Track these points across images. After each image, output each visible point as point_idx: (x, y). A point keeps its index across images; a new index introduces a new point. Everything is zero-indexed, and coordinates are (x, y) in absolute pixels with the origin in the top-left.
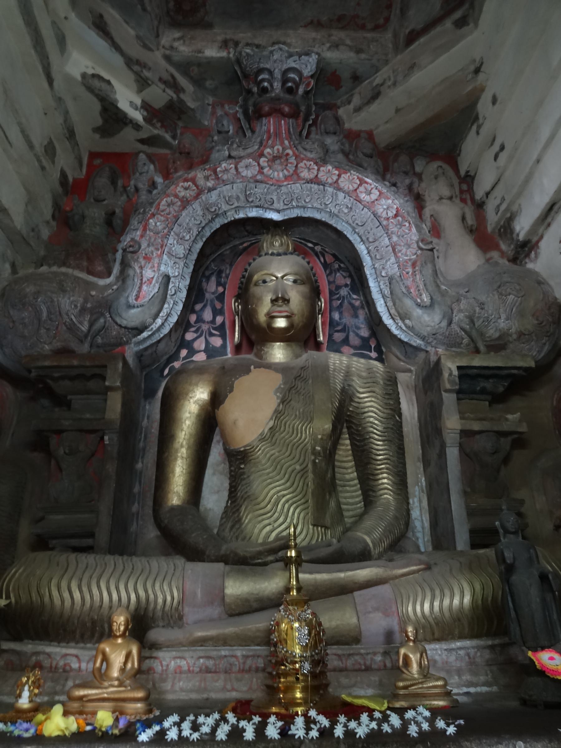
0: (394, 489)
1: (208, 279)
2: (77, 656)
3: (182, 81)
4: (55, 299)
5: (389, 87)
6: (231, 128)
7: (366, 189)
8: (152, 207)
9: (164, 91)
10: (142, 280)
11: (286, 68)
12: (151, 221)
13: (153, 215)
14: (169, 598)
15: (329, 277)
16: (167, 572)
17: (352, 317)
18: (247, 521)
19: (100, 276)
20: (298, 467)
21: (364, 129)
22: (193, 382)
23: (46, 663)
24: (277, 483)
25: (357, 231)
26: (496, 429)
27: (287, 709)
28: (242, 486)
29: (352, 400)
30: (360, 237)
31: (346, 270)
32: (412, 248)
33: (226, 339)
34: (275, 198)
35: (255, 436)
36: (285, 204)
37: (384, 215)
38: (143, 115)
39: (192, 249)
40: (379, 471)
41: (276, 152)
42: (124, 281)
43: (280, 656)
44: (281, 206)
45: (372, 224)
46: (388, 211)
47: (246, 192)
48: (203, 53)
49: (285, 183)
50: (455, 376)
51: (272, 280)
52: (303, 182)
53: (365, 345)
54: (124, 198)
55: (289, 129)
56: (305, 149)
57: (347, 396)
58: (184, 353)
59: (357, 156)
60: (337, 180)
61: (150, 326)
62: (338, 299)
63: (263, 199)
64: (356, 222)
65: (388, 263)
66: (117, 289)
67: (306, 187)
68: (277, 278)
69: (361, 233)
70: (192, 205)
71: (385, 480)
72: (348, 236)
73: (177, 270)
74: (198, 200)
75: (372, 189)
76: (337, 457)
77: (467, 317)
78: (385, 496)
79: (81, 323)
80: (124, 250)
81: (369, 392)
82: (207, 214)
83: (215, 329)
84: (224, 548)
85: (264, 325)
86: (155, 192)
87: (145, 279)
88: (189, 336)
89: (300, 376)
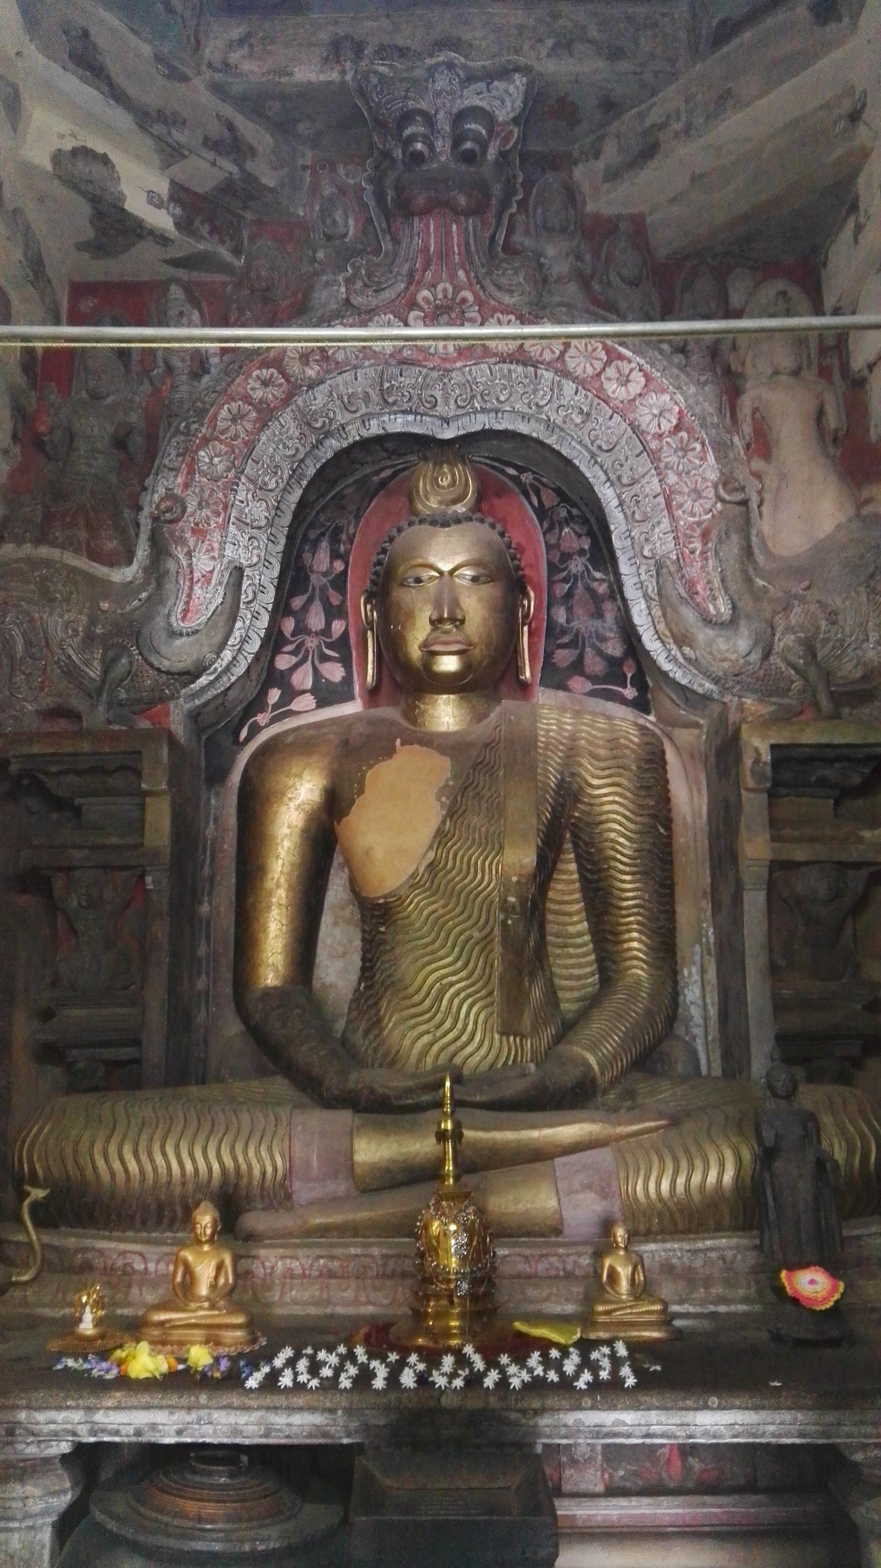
0: (650, 960)
1: (315, 545)
2: (141, 1254)
3: (250, 130)
4: (36, 616)
5: (676, 134)
6: (351, 222)
7: (619, 371)
8: (202, 425)
9: (214, 164)
10: (192, 579)
11: (462, 106)
12: (202, 453)
13: (206, 441)
14: (269, 1169)
15: (548, 536)
16: (264, 1129)
17: (592, 616)
18: (390, 1025)
19: (112, 562)
20: (477, 935)
21: (625, 211)
22: (294, 770)
23: (98, 1262)
24: (441, 963)
25: (599, 460)
26: (836, 857)
27: (436, 1342)
28: (383, 962)
29: (579, 801)
30: (606, 472)
31: (585, 521)
32: (705, 498)
33: (351, 667)
34: (438, 394)
35: (404, 878)
36: (459, 407)
37: (653, 429)
38: (173, 216)
39: (283, 507)
40: (625, 928)
41: (440, 296)
42: (160, 584)
43: (429, 1271)
44: (451, 410)
45: (628, 448)
46: (662, 419)
47: (382, 385)
48: (291, 74)
49: (459, 364)
50: (765, 763)
51: (431, 578)
52: (493, 360)
53: (615, 671)
54: (146, 388)
55: (467, 244)
56: (499, 287)
57: (569, 793)
58: (274, 695)
59: (609, 283)
60: (563, 354)
61: (210, 665)
62: (565, 580)
63: (415, 398)
64: (598, 442)
65: (657, 530)
66: (149, 598)
67: (501, 370)
68: (441, 573)
69: (608, 464)
70: (277, 419)
72: (583, 468)
73: (255, 551)
74: (288, 409)
75: (631, 370)
76: (551, 894)
77: (800, 641)
78: (634, 971)
79: (87, 663)
80: (156, 519)
81: (609, 785)
82: (307, 433)
83: (330, 646)
84: (354, 1076)
85: (419, 664)
86: (206, 379)
87: (197, 575)
88: (283, 662)
89: (482, 762)
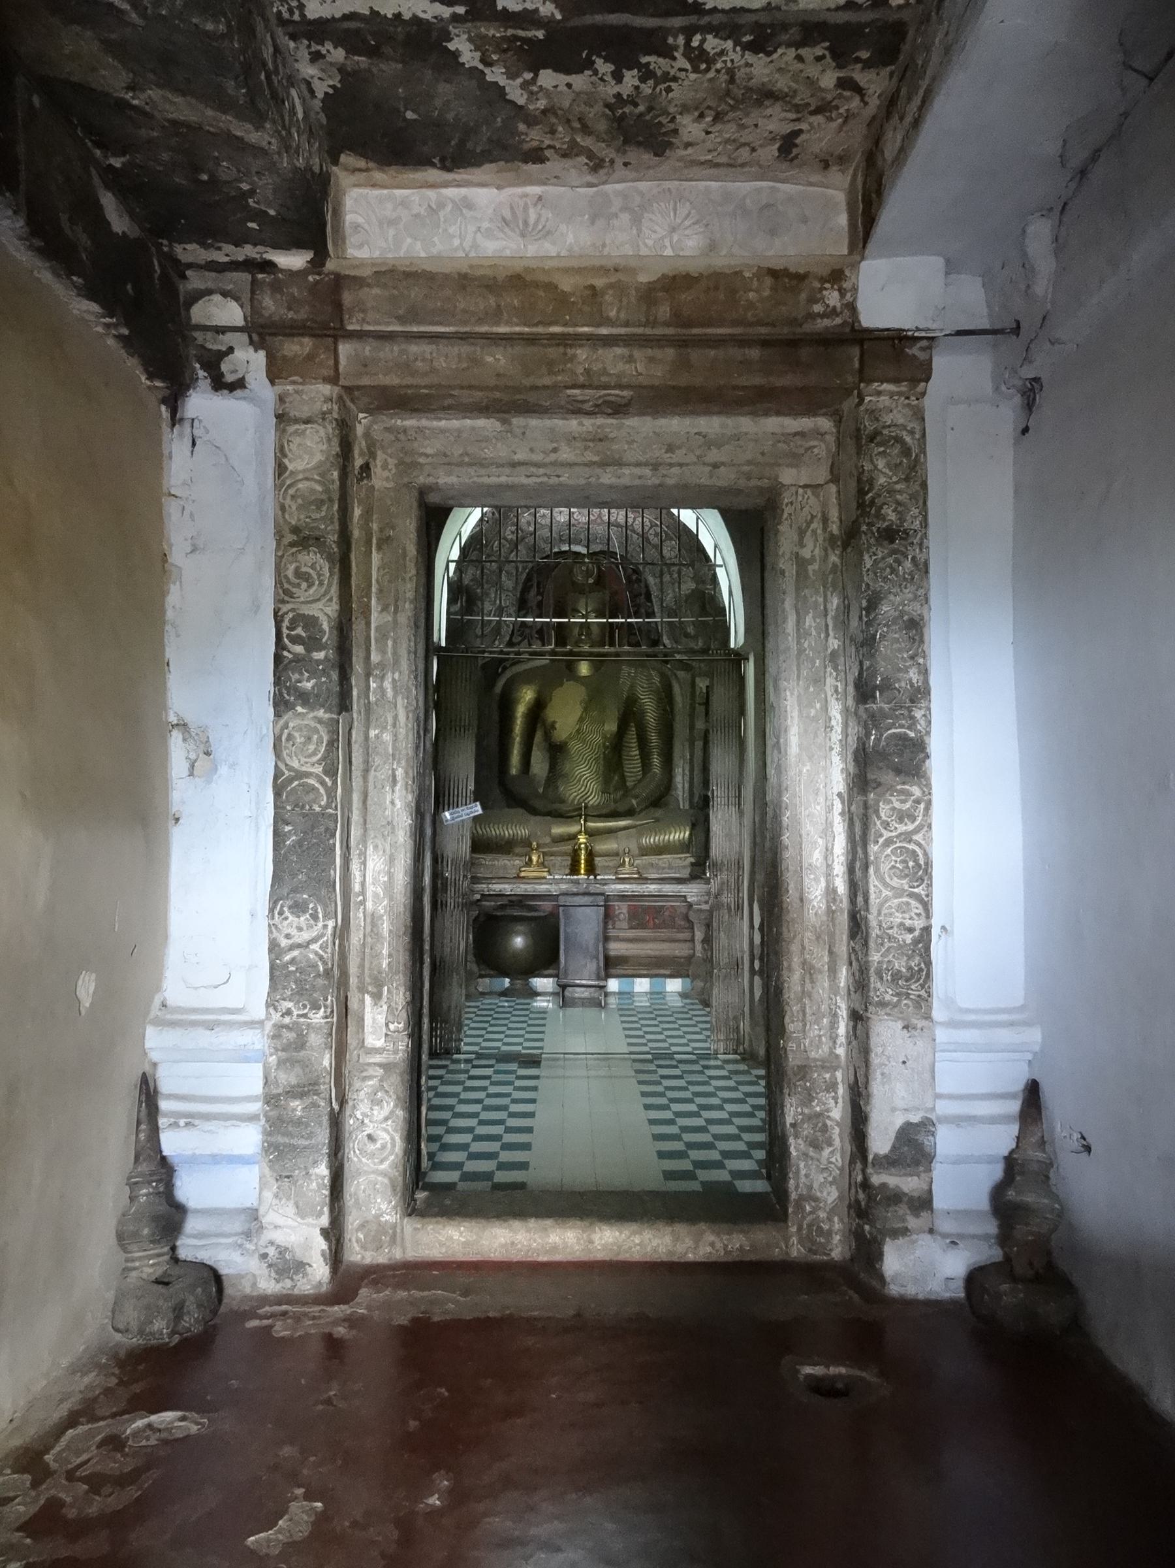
71: (656, 760)
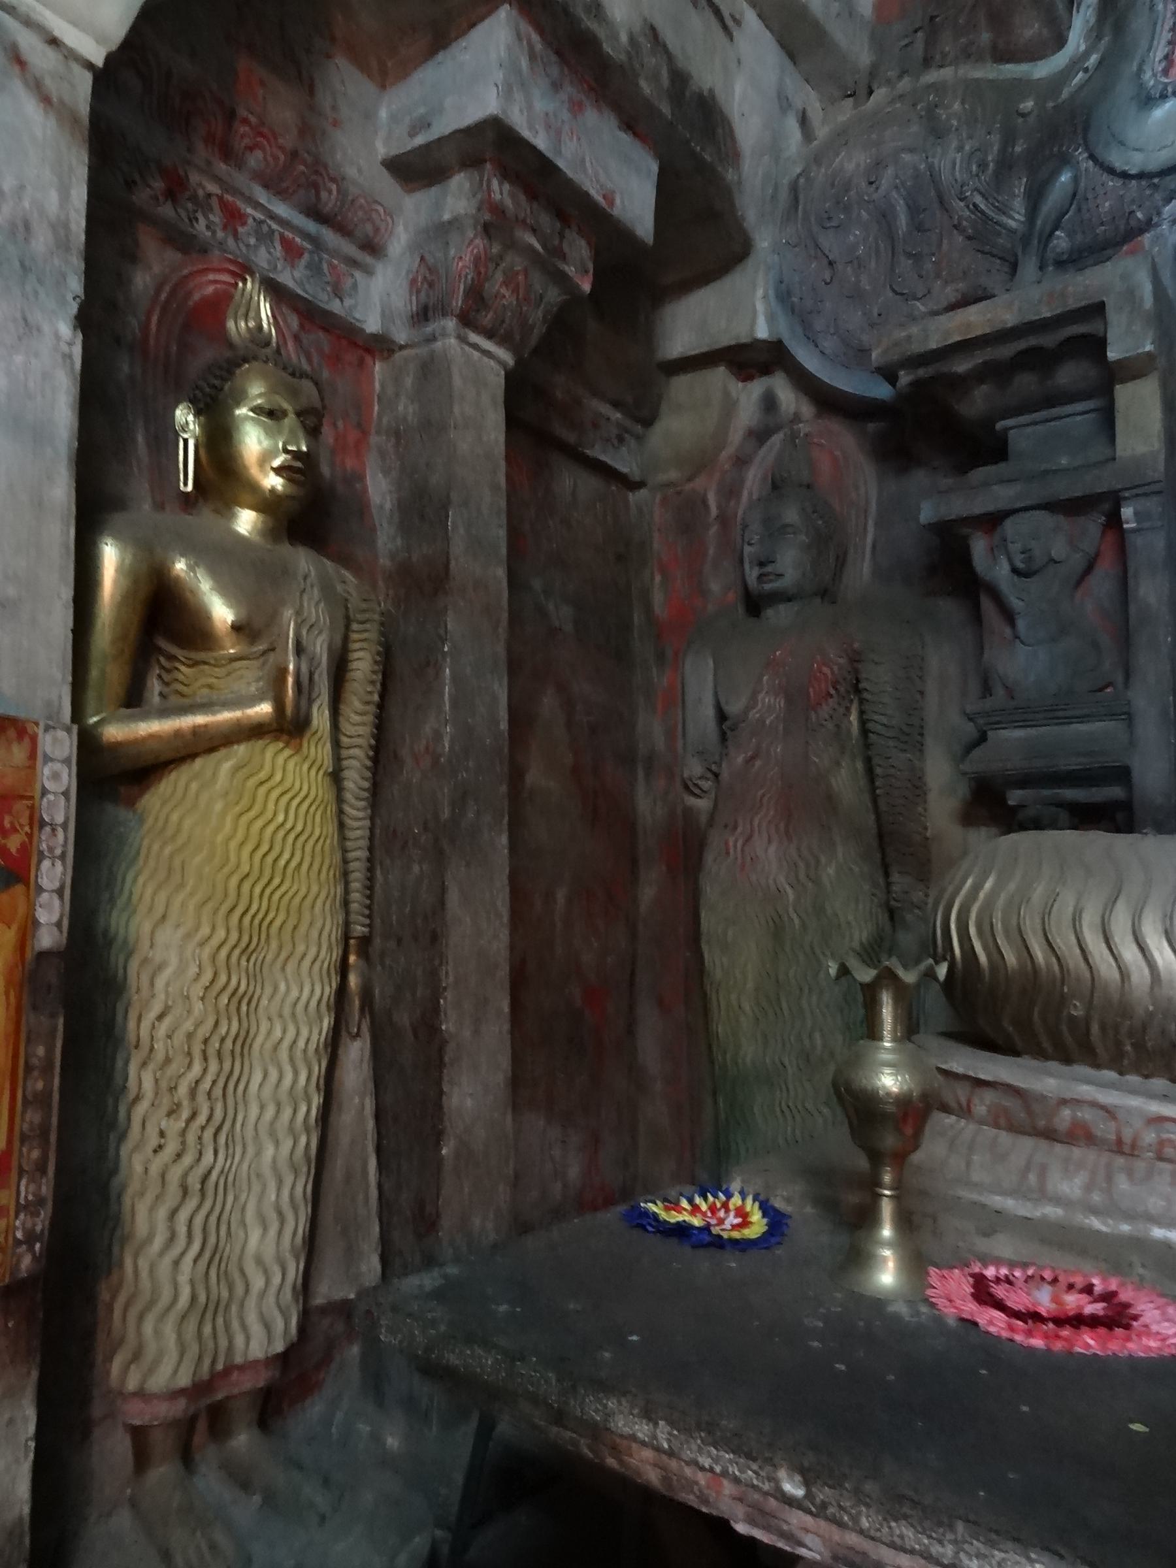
19: (1034, 54)
42: (1119, 29)
66: (1100, 63)
